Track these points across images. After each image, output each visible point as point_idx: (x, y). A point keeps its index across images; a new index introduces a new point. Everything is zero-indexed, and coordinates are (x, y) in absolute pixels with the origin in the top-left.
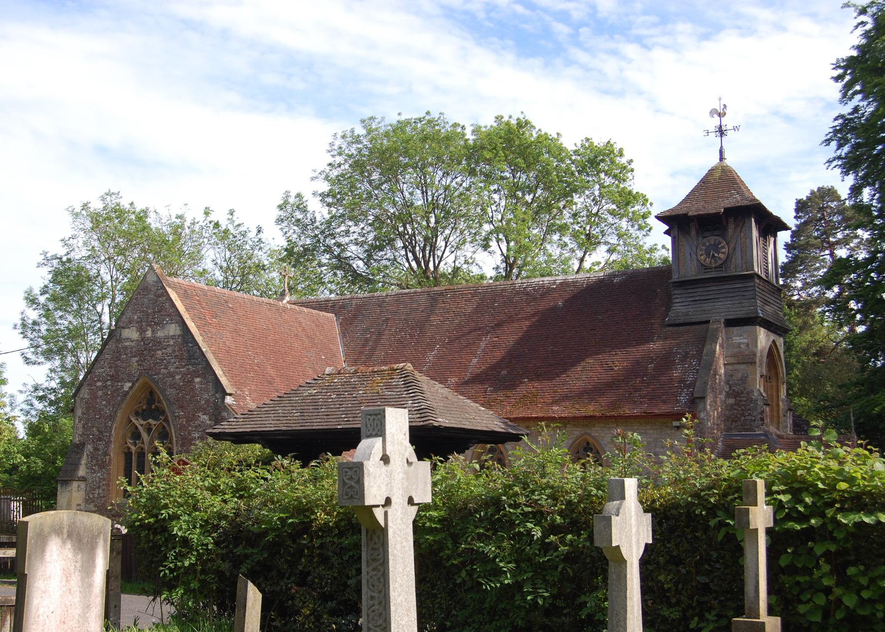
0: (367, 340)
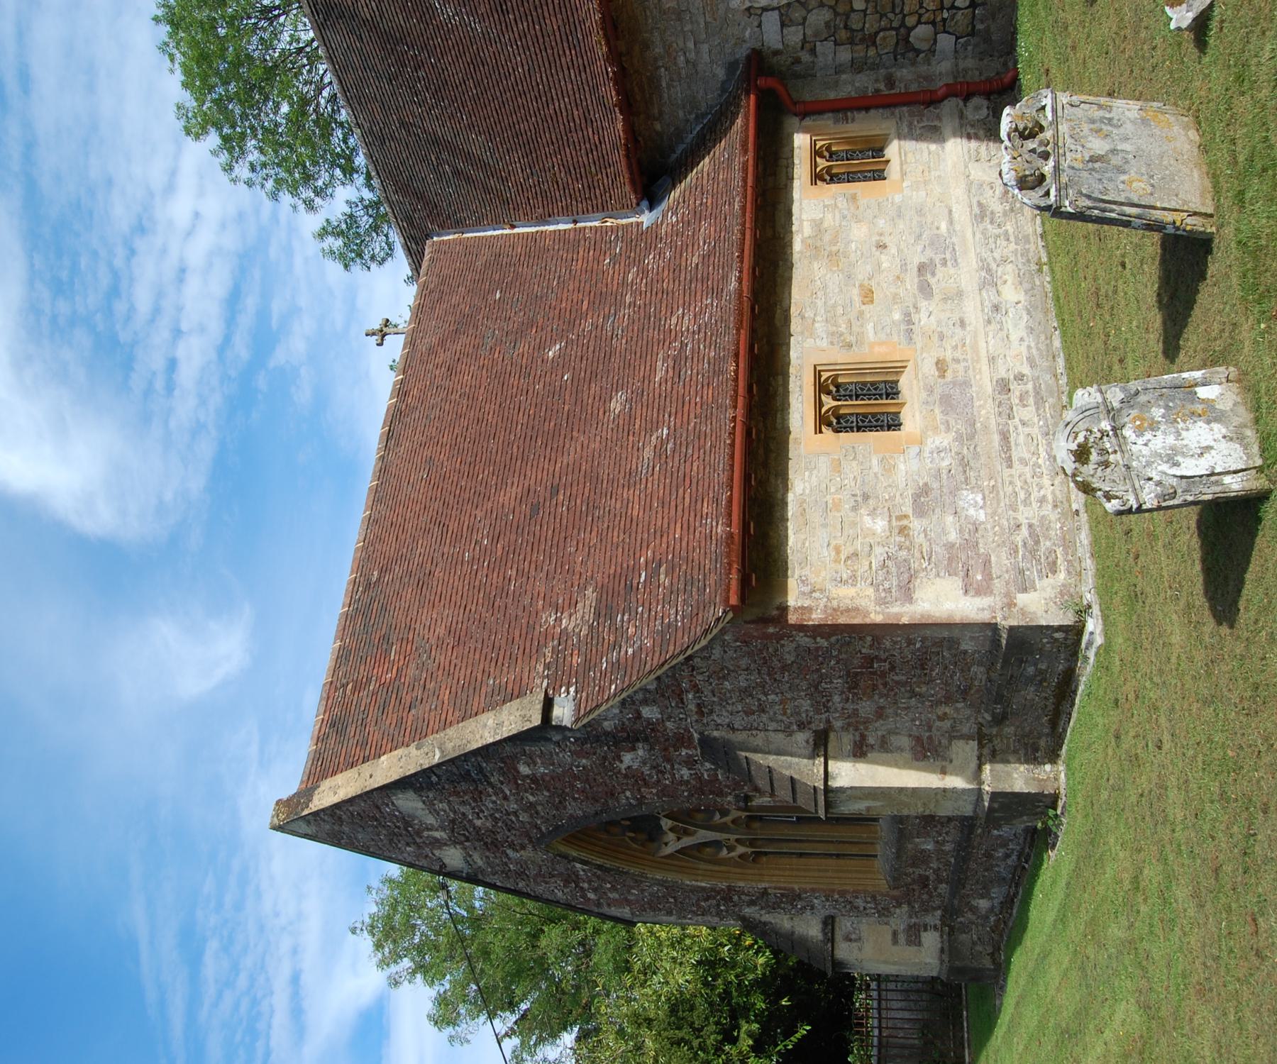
0: (457, 173)
